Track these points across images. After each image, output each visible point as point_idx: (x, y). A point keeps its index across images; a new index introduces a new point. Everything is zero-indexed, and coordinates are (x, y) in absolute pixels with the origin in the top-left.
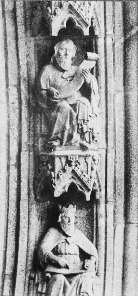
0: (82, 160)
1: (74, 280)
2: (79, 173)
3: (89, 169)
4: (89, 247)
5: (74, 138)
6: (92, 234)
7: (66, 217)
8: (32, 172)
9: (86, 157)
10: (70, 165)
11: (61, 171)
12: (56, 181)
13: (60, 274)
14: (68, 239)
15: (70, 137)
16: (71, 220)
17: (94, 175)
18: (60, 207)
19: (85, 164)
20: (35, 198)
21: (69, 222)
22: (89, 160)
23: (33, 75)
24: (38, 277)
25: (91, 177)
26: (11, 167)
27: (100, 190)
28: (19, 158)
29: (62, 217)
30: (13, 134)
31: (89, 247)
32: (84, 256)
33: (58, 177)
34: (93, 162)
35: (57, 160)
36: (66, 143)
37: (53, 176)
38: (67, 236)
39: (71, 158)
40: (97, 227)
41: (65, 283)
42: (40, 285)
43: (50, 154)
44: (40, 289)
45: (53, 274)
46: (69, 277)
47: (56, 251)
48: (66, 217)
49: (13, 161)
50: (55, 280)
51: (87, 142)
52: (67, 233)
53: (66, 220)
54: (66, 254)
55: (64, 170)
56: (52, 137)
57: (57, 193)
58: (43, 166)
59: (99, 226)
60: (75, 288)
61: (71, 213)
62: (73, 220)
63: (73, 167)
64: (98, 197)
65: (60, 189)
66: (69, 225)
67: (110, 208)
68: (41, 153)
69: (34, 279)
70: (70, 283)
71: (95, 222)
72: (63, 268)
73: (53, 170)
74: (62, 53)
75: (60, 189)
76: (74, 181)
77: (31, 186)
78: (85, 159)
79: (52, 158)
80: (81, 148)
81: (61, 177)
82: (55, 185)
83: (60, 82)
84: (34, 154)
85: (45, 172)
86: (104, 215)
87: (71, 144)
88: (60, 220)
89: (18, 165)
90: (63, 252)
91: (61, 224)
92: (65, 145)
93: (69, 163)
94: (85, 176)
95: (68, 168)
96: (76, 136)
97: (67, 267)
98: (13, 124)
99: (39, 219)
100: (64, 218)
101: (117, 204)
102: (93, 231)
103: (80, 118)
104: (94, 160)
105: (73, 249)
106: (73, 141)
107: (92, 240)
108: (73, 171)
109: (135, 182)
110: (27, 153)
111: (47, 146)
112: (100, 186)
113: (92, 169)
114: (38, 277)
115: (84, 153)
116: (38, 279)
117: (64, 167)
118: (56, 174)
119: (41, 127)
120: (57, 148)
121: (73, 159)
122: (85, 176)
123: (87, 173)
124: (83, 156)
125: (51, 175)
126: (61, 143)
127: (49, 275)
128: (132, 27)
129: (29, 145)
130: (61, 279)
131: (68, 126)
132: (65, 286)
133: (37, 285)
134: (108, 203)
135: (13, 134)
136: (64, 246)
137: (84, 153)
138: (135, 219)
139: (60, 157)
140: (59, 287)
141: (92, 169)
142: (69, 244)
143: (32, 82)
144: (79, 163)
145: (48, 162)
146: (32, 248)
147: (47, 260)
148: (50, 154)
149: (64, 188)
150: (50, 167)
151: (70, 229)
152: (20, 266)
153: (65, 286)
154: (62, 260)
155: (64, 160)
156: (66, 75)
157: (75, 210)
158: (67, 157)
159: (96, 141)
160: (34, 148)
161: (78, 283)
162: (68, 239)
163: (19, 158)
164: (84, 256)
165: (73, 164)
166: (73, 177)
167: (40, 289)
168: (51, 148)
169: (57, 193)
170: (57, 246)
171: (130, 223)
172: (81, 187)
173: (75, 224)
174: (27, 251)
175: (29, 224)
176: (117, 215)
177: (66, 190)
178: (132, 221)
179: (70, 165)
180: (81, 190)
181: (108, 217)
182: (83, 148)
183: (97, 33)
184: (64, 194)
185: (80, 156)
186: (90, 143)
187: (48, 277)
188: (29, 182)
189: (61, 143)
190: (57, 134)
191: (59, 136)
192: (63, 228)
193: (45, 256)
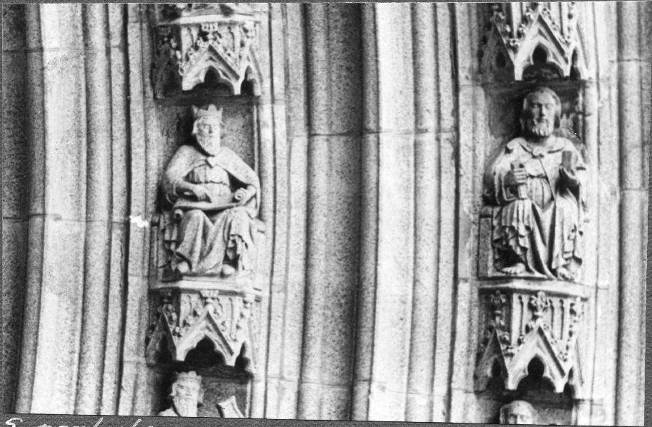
0: (224, 31)
1: (219, 219)
2: (220, 50)
3: (238, 44)
4: (244, 172)
6: (252, 156)
7: (205, 125)
8: (147, 57)
9: (231, 25)
10: (206, 40)
11: (192, 49)
12: (183, 65)
13: (197, 208)
14: (210, 160)
16: (213, 130)
17: (246, 52)
18: (195, 110)
19: (230, 36)
20: (155, 98)
21: (210, 132)
22: (237, 31)
24: (164, 220)
25: (240, 57)
27: (261, 81)
28: (125, 34)
29: (198, 125)
31: (244, 172)
32: (235, 184)
33: (188, 59)
34: (244, 34)
35: (184, 32)
37: (179, 56)
38: (207, 155)
39: (205, 28)
40: (260, 143)
42: (167, 231)
43: (172, 23)
44: (167, 237)
45: (185, 210)
46: (211, 213)
47: (190, 178)
49: (116, 41)
50: (189, 218)
52: (207, 150)
53: (206, 131)
54: (207, 182)
55: (196, 48)
57: (187, 84)
58: (163, 43)
59: (262, 140)
60: (221, 230)
61: (211, 120)
62: (217, 132)
63: (210, 42)
64: (257, 92)
65: (191, 77)
66: (211, 137)
67: (281, 110)
68: (160, 24)
69: (158, 224)
70: (213, 222)
71: (256, 135)
72: (201, 200)
73: (179, 48)
75: (191, 77)
76: (212, 64)
77: (147, 80)
78: (229, 28)
79: (176, 31)
81: (191, 57)
82: (182, 70)
84: (149, 27)
85: (167, 53)
86: (270, 123)
88: (195, 130)
89: (125, 47)
90: (202, 179)
91: (198, 138)
93: (203, 35)
94: (229, 55)
95: (201, 43)
97: (208, 199)
99: (162, 133)
100: (202, 127)
101: (293, 104)
102: (253, 150)
104: (246, 31)
105: (217, 174)
107: (252, 166)
108: (211, 49)
109: (319, 67)
110: (138, 25)
111: (169, 12)
112: (260, 74)
113: (242, 45)
114: (164, 220)
115: (227, 20)
116: (165, 222)
117: (196, 43)
120: (184, 14)
121: (209, 28)
122: (229, 55)
123: (234, 51)
124: (225, 24)
125: (175, 57)
127: (180, 212)
129: (140, 13)
130: (198, 216)
132: (205, 228)
133: (164, 231)
134: (276, 102)
136: (203, 171)
137: (227, 20)
138: (322, 127)
139: (188, 26)
140: (195, 228)
141: (242, 45)
142: (211, 167)
144: (220, 36)
145: (170, 37)
146: (154, 179)
147: (177, 192)
148: (172, 23)
149: (197, 75)
150: (174, 45)
151: (212, 143)
152: (136, 208)
153: (205, 228)
154: (199, 190)
155: (195, 32)
157: (220, 113)
158: (199, 26)
161: (226, 223)
162: (210, 160)
163: (125, 34)
164: (235, 184)
165: (210, 36)
166: (211, 59)
167: (167, 237)
169: (187, 84)
170: (192, 172)
171: (315, 135)
172: (225, 74)
173: (222, 138)
174: (146, 184)
175: (147, 140)
176: (293, 124)
177: (202, 78)
178: (319, 132)
179: (206, 40)
180: (225, 78)
181: (276, 125)
184: (199, 87)
185: (220, 24)
187: (178, 215)
188: (143, 73)
192: (201, 143)
193: (172, 185)
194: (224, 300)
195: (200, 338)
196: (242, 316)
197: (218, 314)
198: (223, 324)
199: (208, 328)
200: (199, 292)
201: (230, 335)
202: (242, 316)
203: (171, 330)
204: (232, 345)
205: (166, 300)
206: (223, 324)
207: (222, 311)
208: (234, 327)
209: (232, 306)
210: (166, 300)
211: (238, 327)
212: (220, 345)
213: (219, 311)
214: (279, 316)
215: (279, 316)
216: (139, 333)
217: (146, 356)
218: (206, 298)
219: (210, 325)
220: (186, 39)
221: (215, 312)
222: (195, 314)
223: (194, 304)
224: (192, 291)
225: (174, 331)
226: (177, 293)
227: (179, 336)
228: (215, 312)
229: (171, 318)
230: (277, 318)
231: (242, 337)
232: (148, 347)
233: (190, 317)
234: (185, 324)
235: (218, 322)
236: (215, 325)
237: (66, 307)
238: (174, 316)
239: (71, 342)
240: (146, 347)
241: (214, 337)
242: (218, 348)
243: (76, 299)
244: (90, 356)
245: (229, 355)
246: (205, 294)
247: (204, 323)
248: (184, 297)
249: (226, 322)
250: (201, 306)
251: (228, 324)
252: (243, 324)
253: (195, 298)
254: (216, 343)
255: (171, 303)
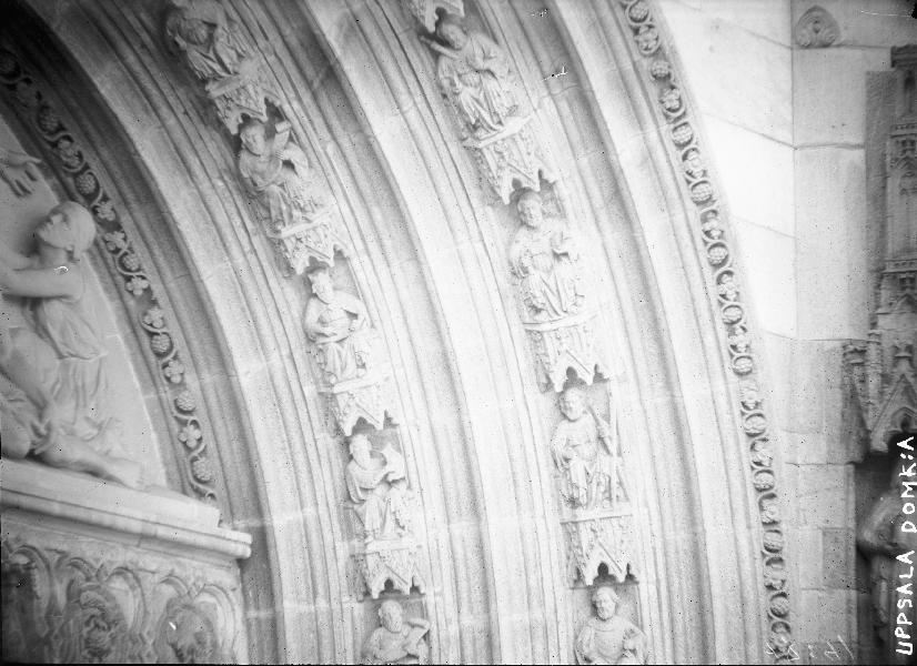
0: (312, 232)
3: (323, 237)
9: (314, 229)
15: (291, 216)
22: (320, 230)
23: (232, 164)
45: (323, 344)
46: (340, 342)
73: (286, 250)
74: (250, 140)
83: (261, 167)
93: (299, 240)
95: (300, 246)
96: (296, 213)
103: (292, 196)
106: (294, 219)
126: (284, 225)
127: (320, 347)
128: (312, 82)
130: (333, 347)
131: (284, 207)
132: (339, 352)
139: (289, 238)
143: (234, 170)
153: (339, 352)
154: (327, 330)
155: (293, 239)
156: (263, 159)
158: (294, 235)
165: (303, 240)
177: (308, 264)
182: (309, 221)
183: (277, 103)
189: (284, 225)
194: (364, 391)
211: (378, 405)
220: (289, 246)
221: (360, 400)
234: (345, 414)
235: (364, 406)
248: (339, 397)
251: (371, 406)
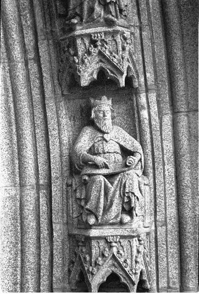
0: (109, 39)
2: (107, 53)
3: (120, 49)
4: (131, 143)
5: (95, 10)
7: (100, 111)
8: (55, 65)
10: (96, 46)
11: (86, 55)
12: (81, 68)
13: (99, 174)
14: (105, 136)
15: (91, 10)
17: (126, 55)
18: (92, 101)
19: (114, 43)
20: (63, 95)
22: (119, 38)
25: (123, 58)
26: (29, 62)
27: (138, 77)
28: (37, 49)
29: (95, 112)
30: (26, 22)
31: (131, 143)
32: (126, 152)
33: (83, 62)
34: (124, 41)
35: (79, 41)
36: (86, 19)
37: (77, 61)
38: (103, 133)
39: (94, 37)
40: (140, 121)
41: (105, 184)
42: (78, 191)
43: (70, 35)
44: (78, 195)
45: (89, 175)
46: (110, 177)
47: (92, 151)
48: (100, 111)
49: (31, 55)
50: (94, 181)
51: (113, 16)
52: (103, 129)
54: (105, 153)
55: (89, 53)
56: (69, 15)
57: (85, 82)
58: (65, 52)
60: (118, 189)
61: (105, 106)
62: (109, 115)
63: (99, 48)
64: (136, 84)
65: (87, 74)
67: (153, 97)
68: (61, 38)
69: (71, 185)
70: (112, 183)
72: (101, 168)
73: (76, 54)
75: (87, 74)
76: (103, 65)
77: (56, 81)
78: (113, 37)
79: (73, 43)
80: (107, 24)
81: (86, 61)
82: (80, 71)
84: (54, 42)
85: (67, 59)
86: (146, 106)
87: (93, 20)
88: (93, 115)
89: (38, 59)
90: (101, 151)
92: (87, 22)
93: (93, 43)
94: (114, 57)
95: (92, 49)
97: (106, 167)
98: (24, 9)
99: (70, 119)
102: (135, 126)
104: (125, 39)
105: (112, 147)
107: (136, 139)
110: (45, 42)
111: (67, 28)
112: (137, 72)
113: (124, 49)
114: (75, 181)
115: (111, 30)
116: (76, 184)
117: (89, 49)
118: (80, 59)
119: (56, 5)
120: (78, 28)
121: (98, 37)
122: (114, 57)
123: (118, 54)
124: (109, 33)
125: (74, 61)
126: (81, 20)
129: (47, 33)
133: (76, 190)
135: (26, 22)
136: (101, 145)
137: (111, 30)
139: (82, 36)
140: (99, 189)
141: (124, 49)
142: (107, 141)
144: (106, 42)
145: (68, 47)
146: (66, 152)
147: (83, 162)
148: (70, 35)
149: (92, 74)
150: (72, 52)
151: (107, 123)
152: (55, 174)
153: (106, 190)
154: (99, 159)
155: (87, 42)
157: (110, 102)
158: (89, 35)
159: (125, 16)
160: (52, 35)
161: (121, 183)
162: (105, 136)
163: (37, 49)
164: (126, 152)
165: (99, 43)
166: (101, 61)
167: (78, 195)
168: (72, 28)
169: (85, 82)
171: (179, 112)
172: (112, 72)
174: (61, 156)
175: (59, 125)
177: (95, 76)
179: (96, 46)
180: (112, 75)
182: (109, 23)
184: (93, 83)
185: (105, 33)
186: (117, 17)
187: (85, 180)
188: (52, 77)
190: (74, 9)
191: (77, 11)
193: (79, 157)
194: (125, 242)
195: (109, 274)
196: (138, 252)
197: (121, 255)
198: (125, 261)
199: (114, 265)
200: (105, 238)
201: (131, 270)
202: (138, 252)
203: (86, 268)
204: (133, 278)
205: (80, 244)
206: (125, 261)
207: (124, 251)
208: (134, 262)
209: (131, 246)
210: (80, 244)
211: (136, 262)
212: (124, 278)
213: (121, 252)
214: (164, 244)
215: (164, 244)
216: (64, 265)
217: (69, 283)
218: (111, 242)
219: (116, 263)
221: (118, 252)
222: (103, 256)
223: (101, 247)
224: (98, 238)
225: (88, 270)
226: (89, 239)
227: (92, 274)
228: (118, 252)
229: (85, 258)
230: (163, 245)
231: (141, 267)
232: (70, 278)
233: (100, 259)
234: (96, 264)
235: (121, 260)
236: (119, 263)
237: (9, 250)
238: (88, 258)
239: (15, 276)
240: (69, 276)
241: (119, 272)
242: (123, 280)
243: (17, 243)
244: (28, 287)
245: (131, 285)
246: (110, 239)
247: (111, 262)
248: (94, 243)
249: (128, 260)
250: (107, 249)
251: (129, 261)
252: (140, 259)
253: (102, 243)
254: (121, 276)
255: (85, 246)
